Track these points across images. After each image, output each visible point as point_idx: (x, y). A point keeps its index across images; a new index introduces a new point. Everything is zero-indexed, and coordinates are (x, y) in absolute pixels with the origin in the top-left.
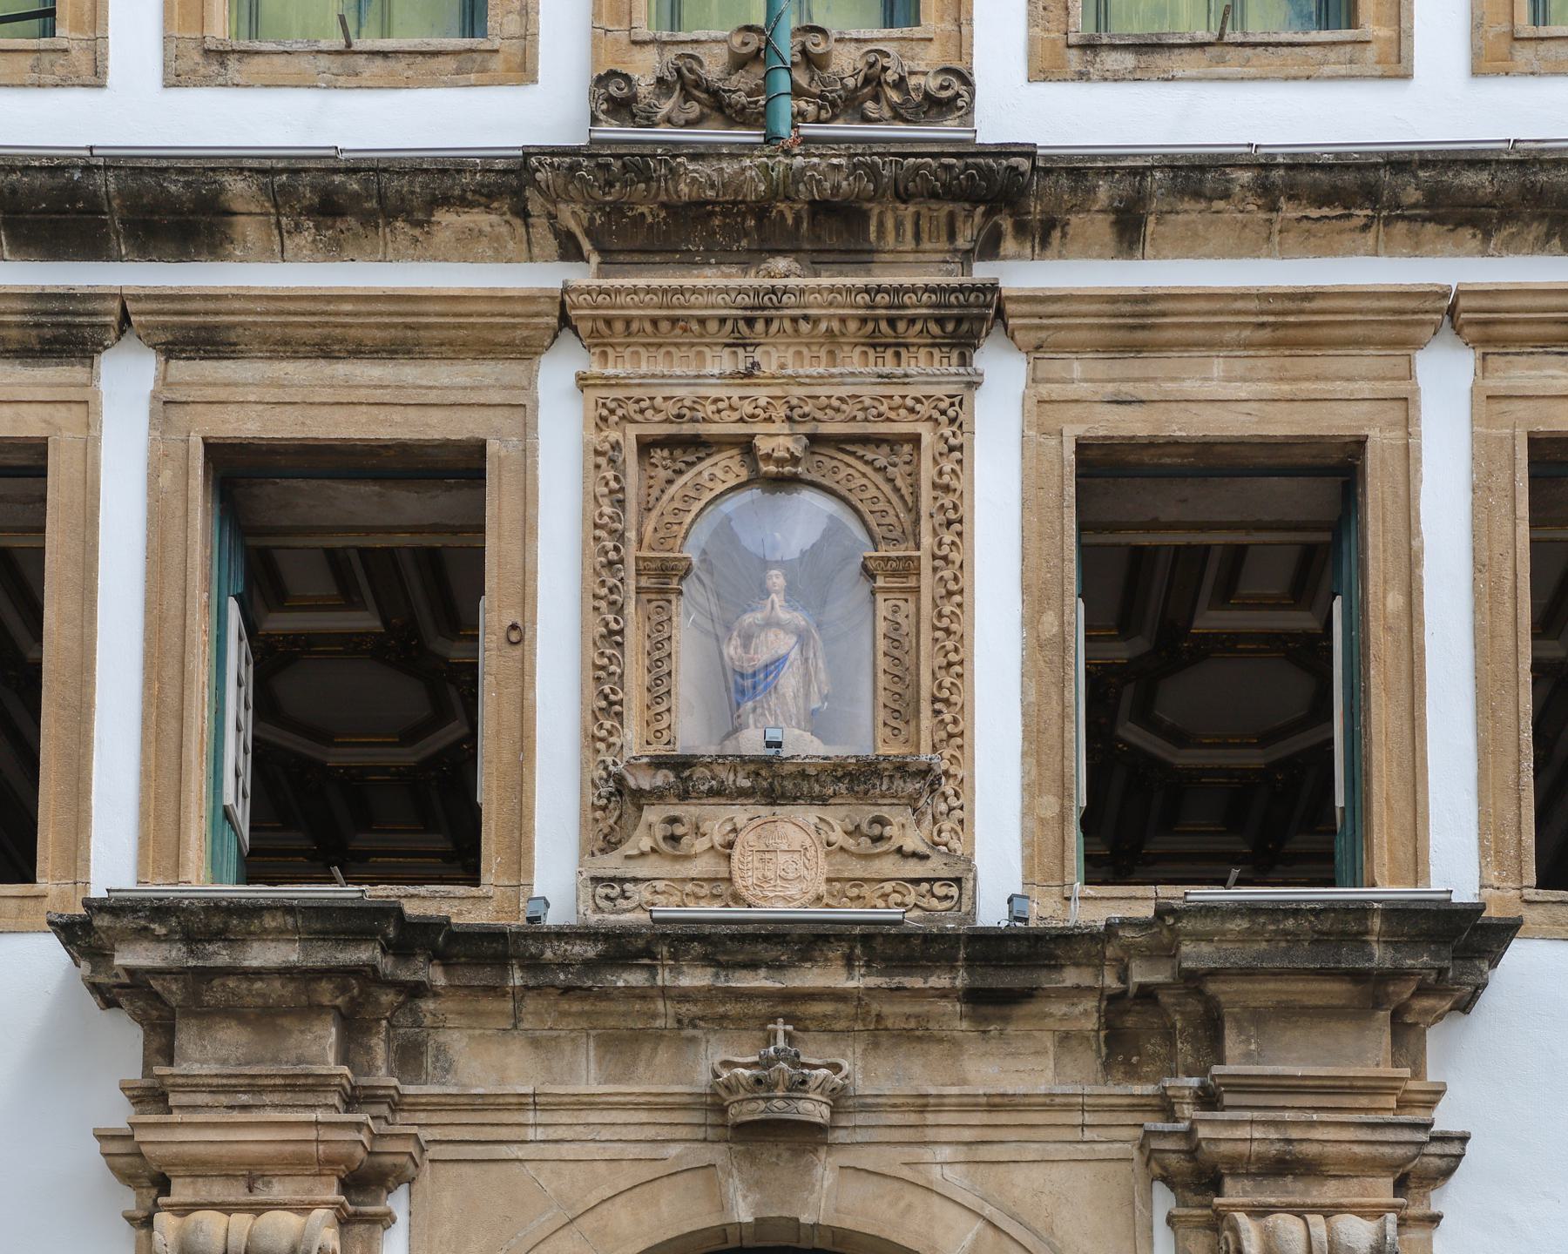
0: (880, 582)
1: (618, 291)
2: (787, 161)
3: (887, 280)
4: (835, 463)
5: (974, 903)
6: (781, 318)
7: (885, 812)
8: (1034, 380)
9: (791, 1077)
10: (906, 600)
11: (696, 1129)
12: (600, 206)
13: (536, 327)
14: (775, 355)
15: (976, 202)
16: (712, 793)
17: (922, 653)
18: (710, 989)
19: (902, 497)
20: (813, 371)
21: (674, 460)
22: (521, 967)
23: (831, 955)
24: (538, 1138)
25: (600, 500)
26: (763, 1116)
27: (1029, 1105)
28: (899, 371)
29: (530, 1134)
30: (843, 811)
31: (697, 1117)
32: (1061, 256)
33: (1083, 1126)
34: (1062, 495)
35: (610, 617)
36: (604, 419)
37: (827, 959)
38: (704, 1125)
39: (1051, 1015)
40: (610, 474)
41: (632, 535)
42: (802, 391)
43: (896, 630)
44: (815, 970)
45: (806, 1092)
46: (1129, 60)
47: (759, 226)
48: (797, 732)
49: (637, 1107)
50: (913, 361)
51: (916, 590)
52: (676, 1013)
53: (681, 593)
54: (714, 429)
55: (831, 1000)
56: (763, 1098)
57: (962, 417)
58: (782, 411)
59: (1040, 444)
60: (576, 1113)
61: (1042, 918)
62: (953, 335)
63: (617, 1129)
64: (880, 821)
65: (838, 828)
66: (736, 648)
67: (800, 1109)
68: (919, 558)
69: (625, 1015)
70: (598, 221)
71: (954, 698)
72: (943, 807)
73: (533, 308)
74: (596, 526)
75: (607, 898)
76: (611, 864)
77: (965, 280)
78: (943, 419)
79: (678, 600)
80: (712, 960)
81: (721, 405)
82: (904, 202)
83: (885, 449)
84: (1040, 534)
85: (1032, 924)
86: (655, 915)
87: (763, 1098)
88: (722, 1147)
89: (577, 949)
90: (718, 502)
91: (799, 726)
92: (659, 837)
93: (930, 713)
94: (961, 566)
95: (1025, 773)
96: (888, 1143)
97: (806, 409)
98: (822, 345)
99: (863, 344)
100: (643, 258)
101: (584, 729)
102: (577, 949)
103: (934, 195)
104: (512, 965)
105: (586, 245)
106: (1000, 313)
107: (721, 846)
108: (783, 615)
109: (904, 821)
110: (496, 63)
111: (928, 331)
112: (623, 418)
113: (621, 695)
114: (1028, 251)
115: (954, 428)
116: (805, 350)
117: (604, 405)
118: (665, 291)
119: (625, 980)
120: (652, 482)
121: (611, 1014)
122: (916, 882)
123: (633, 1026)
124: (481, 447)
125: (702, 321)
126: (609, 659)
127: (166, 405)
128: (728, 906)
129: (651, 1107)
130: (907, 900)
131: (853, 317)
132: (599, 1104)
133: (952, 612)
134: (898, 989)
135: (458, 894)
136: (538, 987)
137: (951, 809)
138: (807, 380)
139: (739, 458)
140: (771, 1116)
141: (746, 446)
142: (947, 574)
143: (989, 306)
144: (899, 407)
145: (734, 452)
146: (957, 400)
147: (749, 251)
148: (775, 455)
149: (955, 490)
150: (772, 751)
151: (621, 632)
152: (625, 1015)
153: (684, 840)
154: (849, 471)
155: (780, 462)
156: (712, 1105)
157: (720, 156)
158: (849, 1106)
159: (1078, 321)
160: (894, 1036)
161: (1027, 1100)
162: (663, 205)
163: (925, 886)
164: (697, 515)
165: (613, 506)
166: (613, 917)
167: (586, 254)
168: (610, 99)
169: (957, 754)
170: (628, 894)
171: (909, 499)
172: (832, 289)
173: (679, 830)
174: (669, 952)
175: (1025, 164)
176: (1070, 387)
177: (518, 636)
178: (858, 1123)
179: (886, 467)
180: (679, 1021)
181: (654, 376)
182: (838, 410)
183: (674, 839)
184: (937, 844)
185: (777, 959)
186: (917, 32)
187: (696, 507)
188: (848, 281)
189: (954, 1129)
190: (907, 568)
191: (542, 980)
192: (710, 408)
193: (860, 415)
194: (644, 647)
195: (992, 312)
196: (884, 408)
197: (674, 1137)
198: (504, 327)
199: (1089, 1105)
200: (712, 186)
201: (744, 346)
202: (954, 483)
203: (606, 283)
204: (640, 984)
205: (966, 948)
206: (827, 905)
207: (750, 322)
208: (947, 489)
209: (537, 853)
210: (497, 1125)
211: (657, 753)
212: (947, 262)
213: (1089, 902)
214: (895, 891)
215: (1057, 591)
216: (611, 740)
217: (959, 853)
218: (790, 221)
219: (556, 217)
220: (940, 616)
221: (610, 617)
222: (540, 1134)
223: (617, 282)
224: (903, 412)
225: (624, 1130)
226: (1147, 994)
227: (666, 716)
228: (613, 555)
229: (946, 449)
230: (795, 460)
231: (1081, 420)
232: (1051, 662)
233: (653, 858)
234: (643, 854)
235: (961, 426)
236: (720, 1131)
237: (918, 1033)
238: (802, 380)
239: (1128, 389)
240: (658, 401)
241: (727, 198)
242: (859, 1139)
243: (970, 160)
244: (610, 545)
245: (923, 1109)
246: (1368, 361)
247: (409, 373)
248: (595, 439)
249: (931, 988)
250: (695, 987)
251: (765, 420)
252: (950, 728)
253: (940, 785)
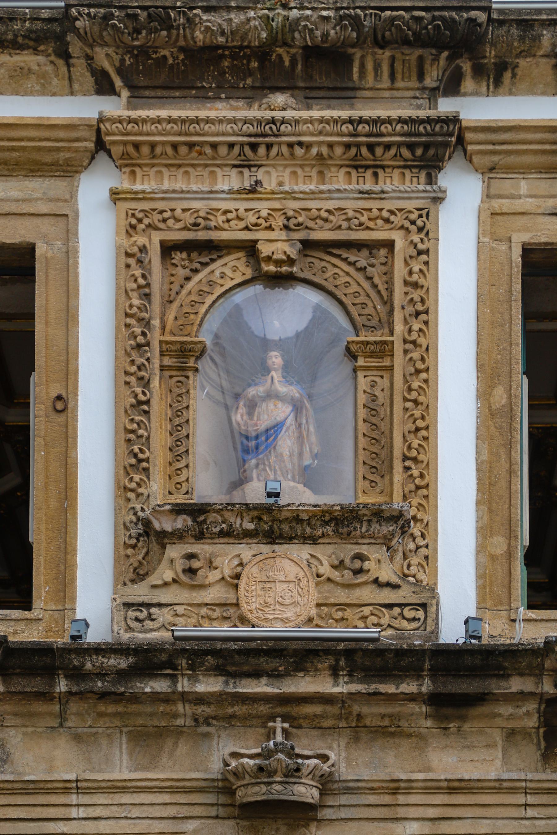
0: (361, 362)
1: (144, 121)
2: (285, 13)
3: (367, 113)
4: (324, 264)
5: (437, 624)
6: (280, 144)
7: (364, 550)
8: (488, 196)
9: (287, 766)
10: (382, 377)
11: (210, 808)
12: (129, 50)
13: (77, 150)
14: (274, 174)
15: (441, 48)
16: (222, 534)
17: (395, 420)
18: (221, 694)
19: (379, 292)
21: (191, 261)
22: (66, 677)
23: (320, 666)
24: (81, 816)
25: (130, 294)
26: (264, 797)
27: (482, 788)
28: (377, 188)
29: (74, 813)
30: (330, 549)
31: (210, 798)
32: (511, 93)
33: (526, 805)
34: (510, 291)
35: (139, 390)
36: (133, 227)
37: (317, 670)
38: (217, 804)
39: (500, 715)
40: (138, 273)
41: (156, 323)
43: (374, 401)
44: (307, 679)
45: (300, 777)
47: (262, 67)
48: (292, 484)
49: (161, 790)
50: (388, 180)
51: (391, 368)
52: (194, 714)
53: (196, 370)
54: (224, 236)
55: (320, 703)
56: (264, 783)
57: (428, 226)
58: (280, 221)
59: (493, 249)
60: (111, 796)
61: (492, 637)
62: (421, 159)
63: (145, 808)
64: (360, 557)
65: (325, 563)
66: (242, 416)
67: (295, 792)
68: (392, 342)
69: (151, 715)
70: (128, 62)
71: (421, 457)
72: (412, 546)
73: (74, 134)
74: (127, 315)
75: (137, 619)
77: (432, 113)
78: (413, 228)
79: (195, 376)
80: (224, 670)
81: (230, 216)
82: (382, 47)
83: (365, 252)
84: (492, 323)
85: (484, 641)
86: (176, 634)
87: (264, 783)
88: (231, 823)
89: (112, 662)
90: (227, 295)
91: (294, 480)
93: (401, 469)
94: (427, 349)
95: (479, 519)
96: (367, 819)
97: (300, 219)
98: (313, 166)
99: (347, 166)
100: (165, 93)
101: (117, 482)
102: (112, 662)
103: (406, 42)
104: (58, 675)
105: (118, 82)
106: (461, 141)
107: (231, 577)
109: (380, 557)
111: (401, 156)
112: (149, 226)
113: (147, 454)
114: (484, 89)
115: (422, 236)
116: (299, 171)
117: (133, 215)
118: (183, 121)
119: (151, 687)
120: (172, 279)
121: (139, 714)
122: (390, 606)
123: (157, 724)
124: (31, 249)
125: (214, 146)
126: (138, 424)
128: (235, 626)
129: (173, 790)
130: (382, 621)
131: (339, 143)
132: (130, 788)
133: (420, 387)
134: (375, 694)
135: (13, 617)
137: (418, 547)
138: (301, 196)
139: (244, 259)
140: (271, 797)
143: (451, 135)
144: (377, 218)
145: (241, 254)
146: (424, 212)
147: (253, 88)
148: (275, 257)
149: (422, 287)
150: (272, 500)
151: (147, 402)
152: (151, 715)
153: (200, 573)
155: (279, 263)
156: (223, 788)
158: (335, 790)
159: (525, 147)
160: (371, 732)
161: (480, 785)
162: (182, 49)
163: (397, 610)
164: (210, 307)
165: (141, 298)
166: (141, 636)
167: (117, 89)
169: (424, 502)
170: (153, 617)
171: (384, 294)
172: (322, 120)
173: (196, 564)
174: (187, 663)
175: (482, 17)
176: (518, 201)
178: (343, 803)
179: (365, 268)
180: (196, 720)
181: (174, 191)
182: (326, 220)
183: (191, 572)
184: (406, 576)
185: (276, 669)
187: (209, 300)
188: (336, 114)
189: (420, 808)
191: (83, 686)
192: (221, 218)
193: (345, 225)
194: (166, 414)
195: (453, 139)
196: (364, 219)
197: (191, 814)
198: (50, 150)
199: (530, 789)
200: (223, 33)
201: (249, 167)
202: (422, 281)
203: (135, 114)
204: (164, 690)
205: (430, 661)
206: (317, 626)
207: (254, 147)
208: (416, 285)
209: (79, 583)
210: (47, 805)
211: (178, 501)
212: (417, 98)
213: (531, 623)
214: (372, 614)
215: (506, 369)
216: (140, 490)
217: (425, 583)
218: (287, 63)
219: (92, 59)
220: (410, 389)
221: (139, 390)
222: (82, 813)
224: (380, 222)
225: (151, 809)
227: (184, 471)
228: (140, 339)
229: (415, 253)
230: (291, 261)
231: (526, 229)
232: (501, 427)
233: (174, 587)
234: (166, 584)
235: (427, 234)
236: (229, 810)
237: (392, 729)
238: (297, 196)
240: (178, 212)
241: (235, 43)
242: (343, 816)
243: (437, 13)
244: (138, 330)
245: (395, 792)
248: (126, 243)
249: (402, 693)
250: (209, 693)
251: (267, 228)
252: (418, 481)
253: (409, 527)
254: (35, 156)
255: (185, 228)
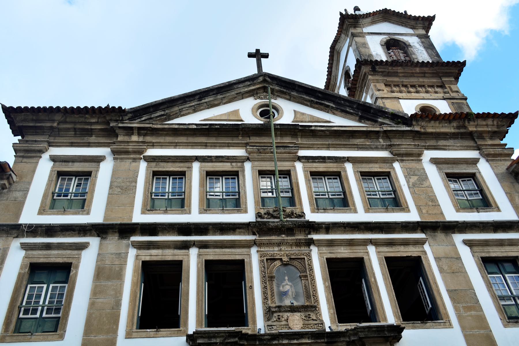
0: (302, 278)
7: (310, 313)
8: (319, 250)
13: (251, 244)
15: (308, 228)
16: (284, 311)
18: (288, 343)
20: (289, 249)
36: (261, 256)
40: (263, 264)
41: (267, 272)
42: (288, 252)
46: (323, 211)
51: (308, 279)
54: (277, 257)
58: (286, 255)
72: (317, 312)
73: (251, 242)
74: (262, 271)
75: (270, 328)
76: (270, 323)
77: (307, 238)
83: (300, 260)
92: (277, 318)
95: (328, 306)
101: (263, 301)
105: (257, 233)
108: (288, 283)
110: (242, 211)
118: (269, 239)
122: (316, 324)
125: (274, 243)
127: (199, 255)
136: (261, 344)
141: (281, 260)
142: (312, 277)
150: (292, 304)
151: (267, 287)
154: (295, 263)
155: (286, 262)
157: (275, 223)
168: (259, 215)
173: (280, 317)
177: (251, 287)
186: (296, 207)
190: (306, 276)
192: (276, 255)
208: (310, 265)
220: (312, 283)
223: (261, 238)
226: (353, 341)
230: (288, 261)
231: (326, 255)
233: (276, 322)
234: (275, 321)
239: (331, 251)
240: (268, 254)
244: (264, 274)
246: (361, 247)
247: (233, 250)
254: (244, 245)
255: (270, 256)
